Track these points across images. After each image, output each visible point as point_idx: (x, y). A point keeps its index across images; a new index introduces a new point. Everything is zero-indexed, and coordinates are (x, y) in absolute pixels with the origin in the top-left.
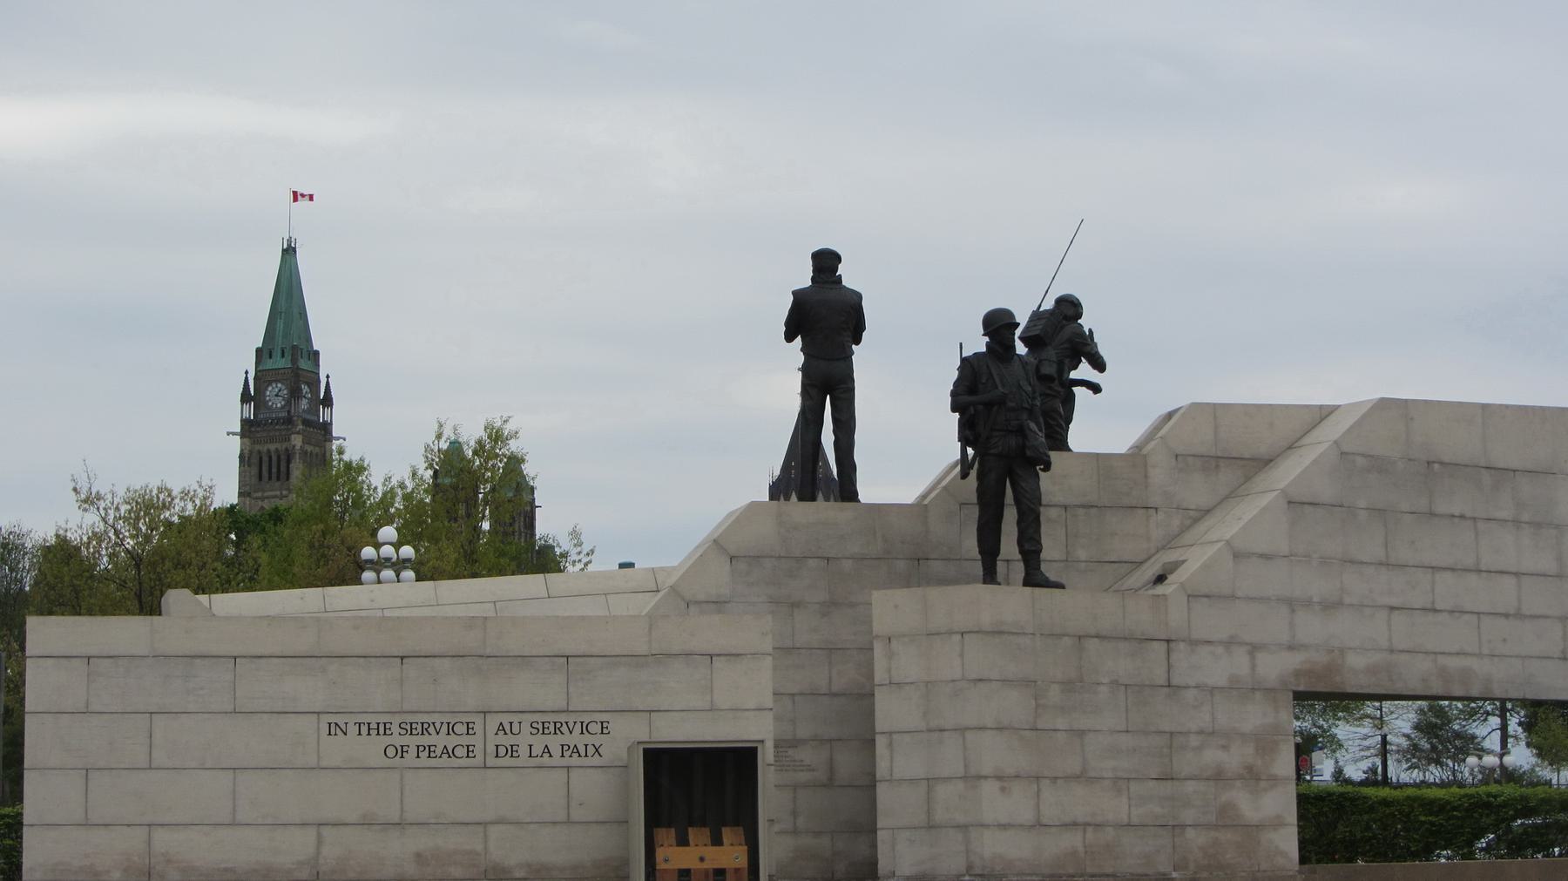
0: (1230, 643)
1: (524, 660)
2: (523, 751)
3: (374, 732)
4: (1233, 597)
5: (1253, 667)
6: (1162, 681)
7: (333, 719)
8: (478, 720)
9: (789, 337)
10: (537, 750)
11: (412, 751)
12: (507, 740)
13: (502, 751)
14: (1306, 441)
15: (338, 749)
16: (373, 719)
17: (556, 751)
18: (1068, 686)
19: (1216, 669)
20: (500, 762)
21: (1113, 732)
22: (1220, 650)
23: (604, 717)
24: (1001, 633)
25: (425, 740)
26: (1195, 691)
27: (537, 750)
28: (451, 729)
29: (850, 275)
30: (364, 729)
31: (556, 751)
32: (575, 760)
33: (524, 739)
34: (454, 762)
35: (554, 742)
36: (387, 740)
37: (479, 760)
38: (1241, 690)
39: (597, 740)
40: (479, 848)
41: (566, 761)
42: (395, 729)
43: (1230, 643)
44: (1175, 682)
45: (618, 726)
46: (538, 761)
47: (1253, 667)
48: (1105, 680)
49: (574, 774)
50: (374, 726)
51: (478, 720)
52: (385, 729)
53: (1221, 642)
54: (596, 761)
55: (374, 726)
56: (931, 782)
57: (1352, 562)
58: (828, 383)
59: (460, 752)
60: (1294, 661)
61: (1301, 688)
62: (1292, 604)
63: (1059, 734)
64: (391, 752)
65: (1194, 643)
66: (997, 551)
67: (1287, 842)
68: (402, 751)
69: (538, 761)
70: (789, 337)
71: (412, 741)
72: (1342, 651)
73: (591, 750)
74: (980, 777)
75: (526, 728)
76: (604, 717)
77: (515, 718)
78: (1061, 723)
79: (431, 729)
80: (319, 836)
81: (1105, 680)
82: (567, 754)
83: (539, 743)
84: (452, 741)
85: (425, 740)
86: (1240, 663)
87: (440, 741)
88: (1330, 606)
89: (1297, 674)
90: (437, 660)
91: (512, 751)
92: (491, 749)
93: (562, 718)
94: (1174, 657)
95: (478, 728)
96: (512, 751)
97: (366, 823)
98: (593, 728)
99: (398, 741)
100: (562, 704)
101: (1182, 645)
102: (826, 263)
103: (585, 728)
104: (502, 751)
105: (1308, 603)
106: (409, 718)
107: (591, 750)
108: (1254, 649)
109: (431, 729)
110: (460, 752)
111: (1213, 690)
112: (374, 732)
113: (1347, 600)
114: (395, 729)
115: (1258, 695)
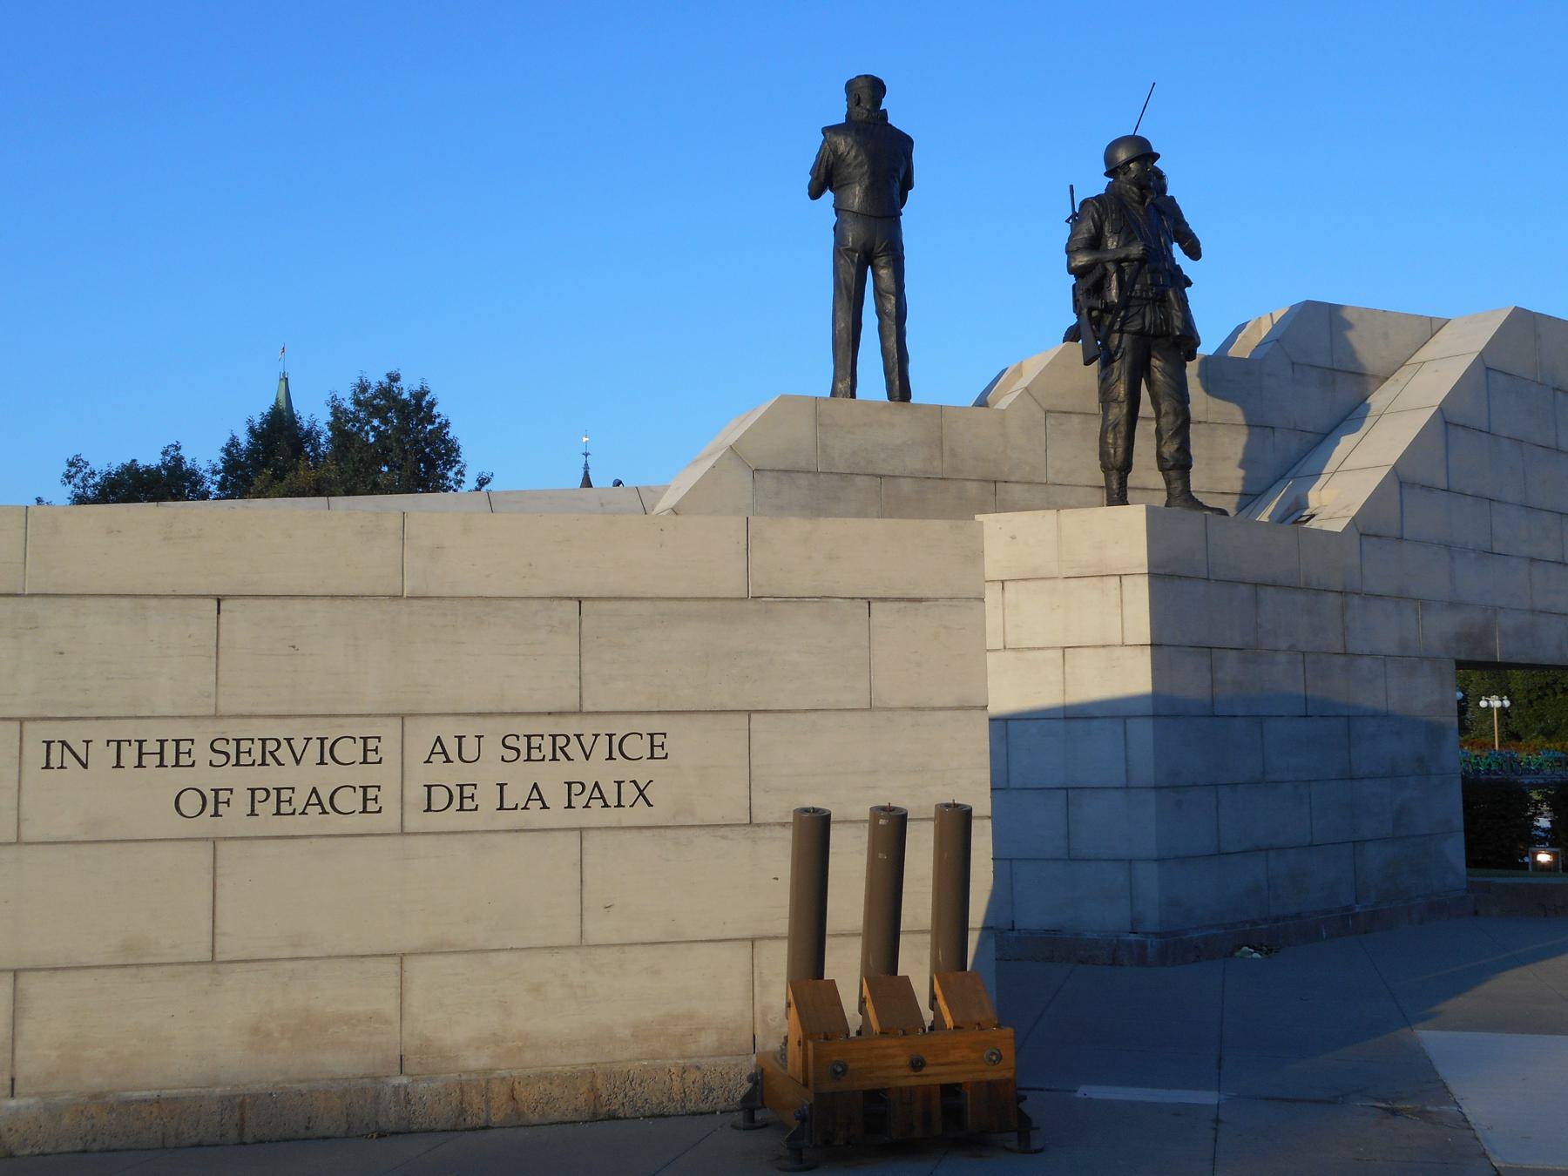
1: (487, 604)
2: (487, 797)
7: (56, 732)
8: (388, 731)
9: (815, 193)
11: (241, 801)
12: (452, 775)
13: (440, 798)
14: (1421, 356)
15: (63, 800)
16: (152, 734)
17: (555, 794)
20: (434, 821)
23: (655, 724)
25: (270, 777)
27: (514, 796)
28: (328, 753)
29: (899, 112)
30: (130, 755)
31: (555, 794)
32: (597, 815)
33: (488, 772)
34: (334, 822)
35: (552, 777)
36: (183, 777)
37: (389, 819)
39: (642, 771)
40: (387, 1005)
41: (578, 817)
42: (201, 753)
45: (683, 738)
46: (516, 819)
48: (1283, 645)
49: (592, 840)
51: (388, 731)
52: (175, 754)
54: (640, 814)
56: (1070, 791)
58: (871, 254)
61: (1462, 657)
64: (191, 803)
66: (1126, 467)
67: (1455, 849)
68: (215, 802)
69: (516, 819)
70: (815, 193)
73: (629, 792)
75: (492, 749)
76: (655, 724)
77: (470, 728)
79: (284, 754)
80: (16, 998)
81: (1283, 645)
82: (578, 802)
83: (520, 778)
84: (328, 778)
85: (270, 777)
87: (303, 777)
90: (298, 605)
92: (416, 794)
93: (570, 726)
95: (389, 749)
96: (461, 797)
97: (133, 962)
98: (631, 747)
99: (207, 778)
100: (571, 702)
103: (616, 748)
104: (440, 798)
106: (235, 730)
107: (629, 792)
109: (284, 754)
114: (201, 753)
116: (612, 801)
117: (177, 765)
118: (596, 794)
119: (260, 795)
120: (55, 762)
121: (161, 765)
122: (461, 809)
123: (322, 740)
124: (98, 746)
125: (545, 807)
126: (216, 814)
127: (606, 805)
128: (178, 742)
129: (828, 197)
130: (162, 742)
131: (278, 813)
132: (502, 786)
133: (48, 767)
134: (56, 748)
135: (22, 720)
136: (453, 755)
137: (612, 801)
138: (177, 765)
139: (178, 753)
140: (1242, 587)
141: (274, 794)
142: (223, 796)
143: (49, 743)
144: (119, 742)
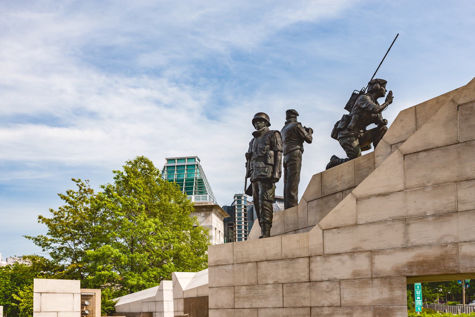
0: (353, 253)
4: (356, 225)
5: (372, 264)
6: (306, 279)
18: (250, 286)
19: (342, 269)
21: (274, 308)
22: (346, 257)
24: (218, 265)
26: (328, 283)
38: (360, 280)
43: (353, 253)
44: (314, 277)
47: (372, 264)
48: (271, 282)
53: (346, 253)
57: (468, 180)
60: (403, 258)
62: (406, 220)
63: (245, 310)
65: (326, 256)
72: (456, 244)
74: (329, 307)
78: (247, 305)
81: (271, 282)
86: (362, 263)
88: (441, 216)
89: (410, 265)
94: (313, 266)
101: (318, 258)
105: (422, 218)
108: (372, 253)
111: (340, 281)
113: (462, 207)
115: (376, 282)
140: (250, 264)
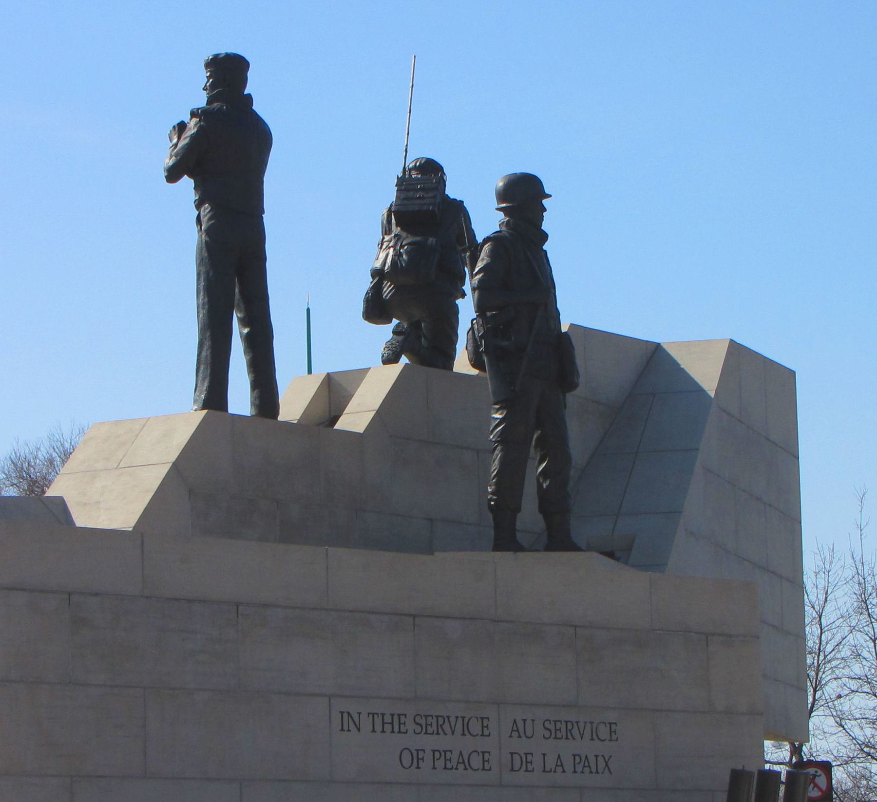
3: (388, 728)
9: (173, 175)
10: (551, 762)
11: (428, 756)
25: (442, 742)
42: (410, 726)
50: (388, 719)
55: (388, 719)
59: (476, 761)
68: (417, 757)
70: (173, 175)
71: (428, 742)
82: (579, 768)
85: (442, 742)
91: (526, 762)
96: (526, 762)
102: (228, 72)
110: (476, 761)
112: (388, 728)
114: (410, 726)
116: (594, 770)
117: (399, 732)
118: (586, 764)
119: (437, 755)
120: (346, 727)
121: (393, 732)
122: (527, 770)
123: (463, 718)
124: (364, 716)
125: (564, 771)
126: (418, 767)
127: (591, 772)
128: (399, 715)
129: (187, 183)
130: (392, 715)
131: (445, 768)
132: (544, 755)
133: (342, 730)
134: (345, 715)
135: (330, 697)
136: (522, 733)
137: (594, 770)
138: (399, 732)
139: (400, 724)
141: (443, 754)
142: (421, 754)
143: (342, 713)
144: (373, 714)
